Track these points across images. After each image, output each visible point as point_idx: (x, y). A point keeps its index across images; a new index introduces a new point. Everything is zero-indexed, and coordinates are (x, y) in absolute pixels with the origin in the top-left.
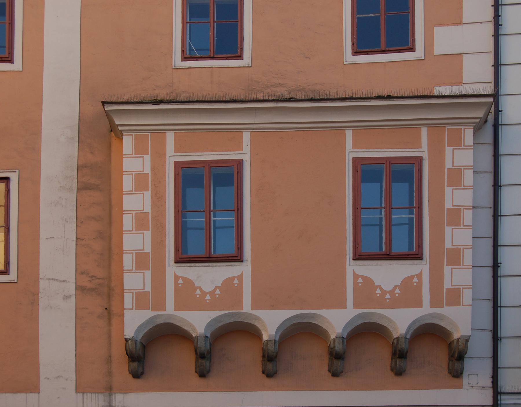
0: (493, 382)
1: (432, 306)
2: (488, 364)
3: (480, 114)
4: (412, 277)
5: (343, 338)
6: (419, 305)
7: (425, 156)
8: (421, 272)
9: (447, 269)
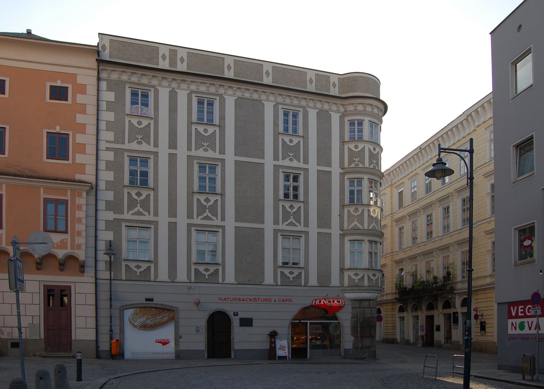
1: (71, 249)
2: (93, 269)
3: (88, 188)
4: (64, 239)
5: (39, 258)
7: (69, 199)
9: (76, 238)
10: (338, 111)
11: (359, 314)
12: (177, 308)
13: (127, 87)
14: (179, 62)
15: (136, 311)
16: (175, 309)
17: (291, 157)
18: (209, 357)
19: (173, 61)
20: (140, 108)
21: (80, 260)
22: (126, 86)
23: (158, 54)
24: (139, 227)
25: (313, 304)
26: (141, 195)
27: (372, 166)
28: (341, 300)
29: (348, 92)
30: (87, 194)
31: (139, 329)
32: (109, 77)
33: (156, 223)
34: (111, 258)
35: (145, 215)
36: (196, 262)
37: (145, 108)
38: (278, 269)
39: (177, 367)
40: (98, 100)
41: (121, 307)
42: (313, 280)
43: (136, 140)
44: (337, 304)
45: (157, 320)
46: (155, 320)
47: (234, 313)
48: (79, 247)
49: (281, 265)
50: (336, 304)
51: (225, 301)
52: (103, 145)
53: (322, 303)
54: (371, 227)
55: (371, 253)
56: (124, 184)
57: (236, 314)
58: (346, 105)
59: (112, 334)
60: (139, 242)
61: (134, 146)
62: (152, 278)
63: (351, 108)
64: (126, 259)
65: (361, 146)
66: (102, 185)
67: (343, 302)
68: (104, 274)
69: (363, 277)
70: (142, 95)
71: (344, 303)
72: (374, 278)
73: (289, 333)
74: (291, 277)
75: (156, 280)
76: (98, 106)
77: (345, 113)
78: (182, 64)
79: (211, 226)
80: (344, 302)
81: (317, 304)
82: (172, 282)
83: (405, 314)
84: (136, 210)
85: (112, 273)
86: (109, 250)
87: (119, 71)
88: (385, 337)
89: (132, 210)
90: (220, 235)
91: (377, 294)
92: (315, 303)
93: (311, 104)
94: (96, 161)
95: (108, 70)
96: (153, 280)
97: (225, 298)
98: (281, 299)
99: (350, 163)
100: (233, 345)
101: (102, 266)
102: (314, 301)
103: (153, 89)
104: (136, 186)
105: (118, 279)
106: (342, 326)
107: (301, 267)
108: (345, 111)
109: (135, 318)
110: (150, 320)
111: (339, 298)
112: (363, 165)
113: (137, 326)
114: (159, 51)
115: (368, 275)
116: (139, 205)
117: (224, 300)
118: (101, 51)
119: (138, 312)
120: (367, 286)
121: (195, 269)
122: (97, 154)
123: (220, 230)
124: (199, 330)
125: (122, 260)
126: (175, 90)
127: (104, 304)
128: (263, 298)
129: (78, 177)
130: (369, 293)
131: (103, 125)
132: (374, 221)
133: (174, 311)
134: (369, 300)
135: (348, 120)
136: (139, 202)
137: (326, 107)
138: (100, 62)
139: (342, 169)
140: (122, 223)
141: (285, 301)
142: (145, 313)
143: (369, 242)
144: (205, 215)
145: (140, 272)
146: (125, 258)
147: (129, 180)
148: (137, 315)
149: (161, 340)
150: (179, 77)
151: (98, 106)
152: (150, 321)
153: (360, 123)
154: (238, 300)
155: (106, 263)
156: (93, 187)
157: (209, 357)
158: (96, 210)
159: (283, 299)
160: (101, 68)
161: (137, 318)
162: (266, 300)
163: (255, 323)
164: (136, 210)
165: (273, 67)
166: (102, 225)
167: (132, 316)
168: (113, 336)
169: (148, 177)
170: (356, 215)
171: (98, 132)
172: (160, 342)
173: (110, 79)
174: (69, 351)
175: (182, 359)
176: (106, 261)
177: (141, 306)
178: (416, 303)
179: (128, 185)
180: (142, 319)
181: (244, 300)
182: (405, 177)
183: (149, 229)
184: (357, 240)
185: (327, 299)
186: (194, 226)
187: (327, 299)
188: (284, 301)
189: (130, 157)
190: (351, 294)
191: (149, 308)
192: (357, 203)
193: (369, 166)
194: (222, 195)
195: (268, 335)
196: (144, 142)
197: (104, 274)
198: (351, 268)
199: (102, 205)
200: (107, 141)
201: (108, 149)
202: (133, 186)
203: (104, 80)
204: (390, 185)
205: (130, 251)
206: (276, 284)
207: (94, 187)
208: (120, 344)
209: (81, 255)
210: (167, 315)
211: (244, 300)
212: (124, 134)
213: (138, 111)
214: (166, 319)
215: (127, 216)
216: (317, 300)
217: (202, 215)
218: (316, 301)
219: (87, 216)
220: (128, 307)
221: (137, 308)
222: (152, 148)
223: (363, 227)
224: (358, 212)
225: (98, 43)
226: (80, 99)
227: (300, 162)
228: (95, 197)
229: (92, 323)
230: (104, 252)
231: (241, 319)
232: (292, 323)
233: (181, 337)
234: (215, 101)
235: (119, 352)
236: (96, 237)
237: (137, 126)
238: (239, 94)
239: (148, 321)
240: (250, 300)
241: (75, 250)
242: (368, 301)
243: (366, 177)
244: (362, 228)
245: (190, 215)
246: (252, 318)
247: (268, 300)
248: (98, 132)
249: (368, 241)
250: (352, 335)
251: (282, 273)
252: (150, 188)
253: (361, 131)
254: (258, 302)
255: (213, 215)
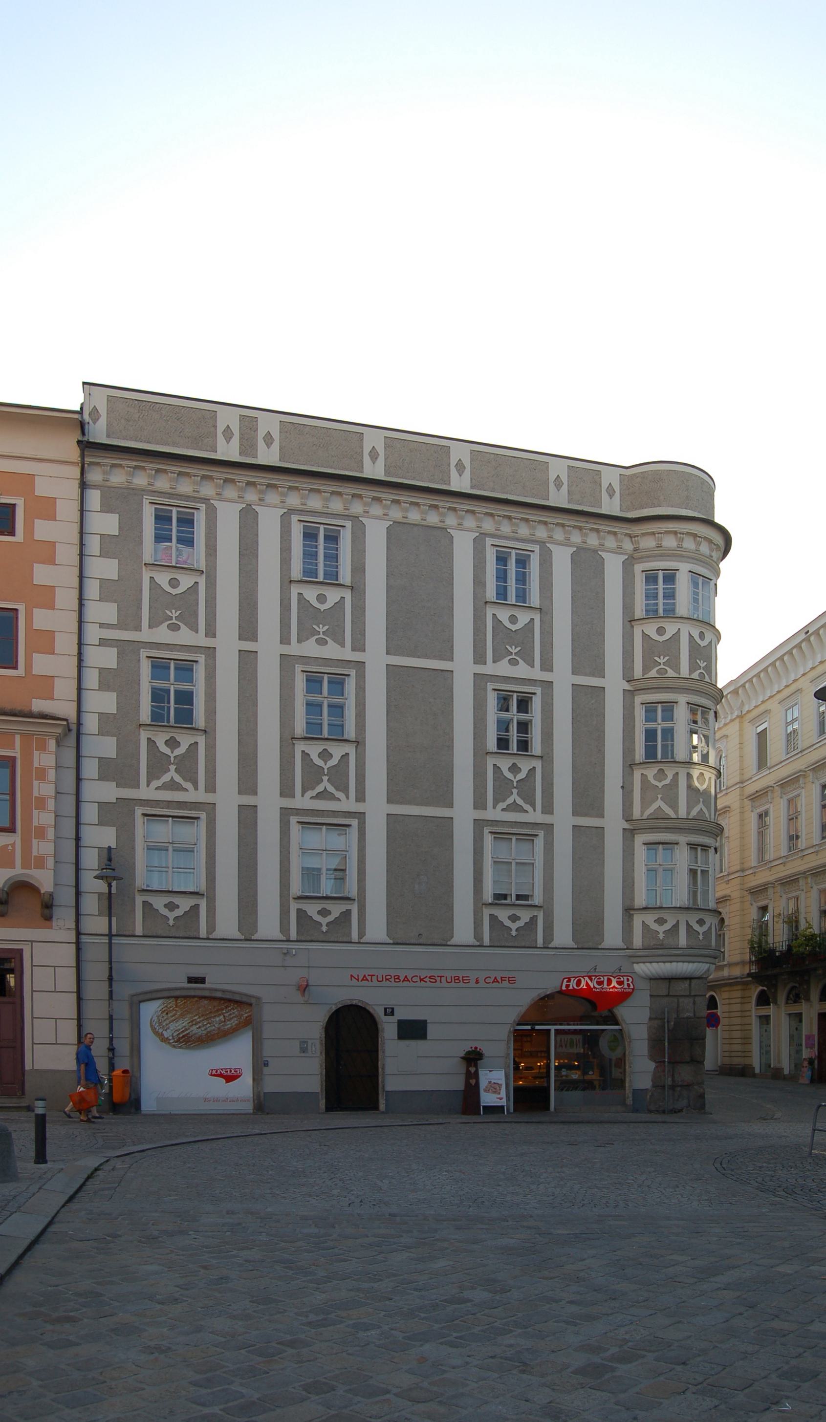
0: (76, 925)
2: (73, 911)
4: (8, 845)
6: (13, 866)
7: (18, 756)
8: (15, 842)
9: (35, 842)
10: (619, 551)
11: (666, 1009)
12: (258, 999)
13: (146, 503)
14: (261, 444)
15: (166, 1006)
16: (253, 1001)
17: (513, 656)
18: (329, 1108)
19: (248, 443)
20: (174, 549)
21: (42, 892)
22: (144, 500)
23: (215, 427)
24: (173, 817)
25: (564, 988)
26: (178, 744)
27: (695, 675)
28: (625, 978)
29: (642, 507)
30: (58, 744)
31: (174, 1046)
32: (106, 481)
33: (210, 808)
34: (111, 886)
35: (186, 790)
36: (299, 894)
37: (185, 550)
38: (484, 909)
39: (257, 1131)
40: (82, 533)
41: (133, 996)
42: (563, 935)
43: (167, 620)
44: (617, 988)
45: (214, 1026)
46: (209, 1025)
47: (385, 1009)
48: (40, 863)
49: (490, 901)
50: (614, 987)
51: (365, 983)
52: (93, 634)
53: (583, 983)
54: (694, 813)
55: (693, 872)
56: (139, 719)
57: (389, 1012)
58: (638, 536)
59: (113, 1058)
60: (174, 850)
61: (162, 635)
62: (203, 932)
63: (648, 543)
64: (145, 888)
65: (671, 629)
66: (91, 724)
67: (629, 982)
68: (96, 924)
69: (676, 926)
70: (179, 520)
71: (632, 987)
72: (701, 930)
73: (508, 1054)
74: (514, 926)
75: (211, 937)
76: (82, 545)
77: (636, 555)
78: (268, 448)
79: (334, 813)
80: (632, 982)
81: (571, 988)
82: (246, 940)
83: (771, 1010)
84: (166, 778)
85: (114, 919)
86: (106, 869)
87: (127, 467)
88: (727, 1061)
89: (158, 778)
90: (354, 832)
91: (707, 966)
92: (567, 986)
93: (559, 535)
94: (76, 668)
95: (104, 465)
96: (205, 937)
97: (365, 976)
98: (490, 977)
99: (646, 669)
100: (383, 1082)
101: (90, 904)
102: (566, 980)
103: (204, 505)
104: (166, 724)
105: (127, 933)
106: (629, 1037)
107: (537, 904)
108: (635, 550)
109: (165, 1020)
110: (198, 1026)
111: (622, 975)
112: (677, 673)
113: (170, 1040)
114: (216, 421)
115: (687, 921)
116: (172, 768)
117: (363, 980)
118: (88, 423)
119: (171, 1007)
120: (685, 947)
121: (299, 911)
122: (80, 654)
123: (355, 823)
124: (307, 1048)
125: (136, 890)
126: (254, 507)
127: (96, 990)
128: (449, 974)
129: (38, 705)
130: (689, 962)
131: (93, 590)
132: (701, 800)
133: (251, 1005)
134: (689, 979)
135: (643, 571)
136: (172, 762)
137: (593, 541)
138: (87, 446)
139: (628, 681)
140: (136, 808)
141: (500, 981)
142: (186, 1011)
143: (689, 846)
144: (320, 788)
145: (176, 918)
146: (143, 888)
147: (152, 710)
148: (169, 1015)
149: (222, 1069)
150: (262, 479)
151: (82, 545)
152: (198, 1028)
153: (670, 577)
154: (395, 979)
155: (99, 899)
156: (71, 728)
157: (329, 1108)
158: (79, 780)
159: (495, 978)
160: (87, 460)
161: (168, 1021)
162: (457, 979)
163: (431, 1030)
164: (166, 778)
165: (472, 451)
166: (90, 813)
167: (158, 1017)
168: (117, 1061)
169: (192, 705)
170: (660, 785)
171: (81, 605)
172: (221, 1075)
173: (108, 484)
174: (18, 1094)
175: (268, 1114)
176: (100, 894)
177: (177, 993)
178: (797, 985)
179: (149, 722)
180: (181, 1024)
181: (408, 980)
182: (771, 697)
183: (196, 821)
184: (663, 843)
185: (593, 978)
186: (297, 815)
187: (593, 978)
188: (498, 982)
189: (153, 659)
190: (648, 964)
191: (196, 999)
192: (662, 759)
193: (690, 675)
194: (359, 743)
195: (462, 1058)
196: (184, 625)
197: (96, 924)
198: (649, 906)
199: (90, 769)
200: (102, 625)
201: (103, 642)
202: (160, 724)
203: (95, 487)
204: (738, 717)
205: (153, 871)
206: (478, 944)
207: (74, 727)
208: (132, 1078)
209: (45, 880)
210: (234, 1015)
211: (408, 980)
212: (139, 607)
213: (171, 557)
214: (234, 1022)
215: (146, 792)
216: (572, 979)
217: (313, 789)
218: (569, 981)
219: (58, 793)
220: (149, 996)
221: (168, 998)
222: (200, 639)
223: (676, 812)
224: (665, 779)
225: (82, 404)
226: (43, 530)
227: (533, 666)
228: (75, 750)
229: (69, 1032)
230: (96, 873)
231: (401, 1024)
232: (516, 1030)
233: (267, 1064)
234: (341, 531)
235: (130, 1097)
236: (78, 839)
237: (169, 589)
238: (396, 514)
239: (194, 1027)
240: (421, 980)
241: (31, 869)
242: (688, 982)
243: (682, 699)
244: (673, 815)
245: (287, 791)
246: (426, 1021)
247: (461, 979)
248: (81, 605)
249: (688, 844)
250: (652, 1057)
251: (492, 917)
252: (198, 729)
253: (670, 595)
254: (438, 984)
255: (337, 790)
